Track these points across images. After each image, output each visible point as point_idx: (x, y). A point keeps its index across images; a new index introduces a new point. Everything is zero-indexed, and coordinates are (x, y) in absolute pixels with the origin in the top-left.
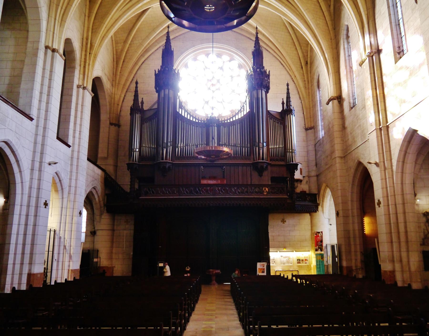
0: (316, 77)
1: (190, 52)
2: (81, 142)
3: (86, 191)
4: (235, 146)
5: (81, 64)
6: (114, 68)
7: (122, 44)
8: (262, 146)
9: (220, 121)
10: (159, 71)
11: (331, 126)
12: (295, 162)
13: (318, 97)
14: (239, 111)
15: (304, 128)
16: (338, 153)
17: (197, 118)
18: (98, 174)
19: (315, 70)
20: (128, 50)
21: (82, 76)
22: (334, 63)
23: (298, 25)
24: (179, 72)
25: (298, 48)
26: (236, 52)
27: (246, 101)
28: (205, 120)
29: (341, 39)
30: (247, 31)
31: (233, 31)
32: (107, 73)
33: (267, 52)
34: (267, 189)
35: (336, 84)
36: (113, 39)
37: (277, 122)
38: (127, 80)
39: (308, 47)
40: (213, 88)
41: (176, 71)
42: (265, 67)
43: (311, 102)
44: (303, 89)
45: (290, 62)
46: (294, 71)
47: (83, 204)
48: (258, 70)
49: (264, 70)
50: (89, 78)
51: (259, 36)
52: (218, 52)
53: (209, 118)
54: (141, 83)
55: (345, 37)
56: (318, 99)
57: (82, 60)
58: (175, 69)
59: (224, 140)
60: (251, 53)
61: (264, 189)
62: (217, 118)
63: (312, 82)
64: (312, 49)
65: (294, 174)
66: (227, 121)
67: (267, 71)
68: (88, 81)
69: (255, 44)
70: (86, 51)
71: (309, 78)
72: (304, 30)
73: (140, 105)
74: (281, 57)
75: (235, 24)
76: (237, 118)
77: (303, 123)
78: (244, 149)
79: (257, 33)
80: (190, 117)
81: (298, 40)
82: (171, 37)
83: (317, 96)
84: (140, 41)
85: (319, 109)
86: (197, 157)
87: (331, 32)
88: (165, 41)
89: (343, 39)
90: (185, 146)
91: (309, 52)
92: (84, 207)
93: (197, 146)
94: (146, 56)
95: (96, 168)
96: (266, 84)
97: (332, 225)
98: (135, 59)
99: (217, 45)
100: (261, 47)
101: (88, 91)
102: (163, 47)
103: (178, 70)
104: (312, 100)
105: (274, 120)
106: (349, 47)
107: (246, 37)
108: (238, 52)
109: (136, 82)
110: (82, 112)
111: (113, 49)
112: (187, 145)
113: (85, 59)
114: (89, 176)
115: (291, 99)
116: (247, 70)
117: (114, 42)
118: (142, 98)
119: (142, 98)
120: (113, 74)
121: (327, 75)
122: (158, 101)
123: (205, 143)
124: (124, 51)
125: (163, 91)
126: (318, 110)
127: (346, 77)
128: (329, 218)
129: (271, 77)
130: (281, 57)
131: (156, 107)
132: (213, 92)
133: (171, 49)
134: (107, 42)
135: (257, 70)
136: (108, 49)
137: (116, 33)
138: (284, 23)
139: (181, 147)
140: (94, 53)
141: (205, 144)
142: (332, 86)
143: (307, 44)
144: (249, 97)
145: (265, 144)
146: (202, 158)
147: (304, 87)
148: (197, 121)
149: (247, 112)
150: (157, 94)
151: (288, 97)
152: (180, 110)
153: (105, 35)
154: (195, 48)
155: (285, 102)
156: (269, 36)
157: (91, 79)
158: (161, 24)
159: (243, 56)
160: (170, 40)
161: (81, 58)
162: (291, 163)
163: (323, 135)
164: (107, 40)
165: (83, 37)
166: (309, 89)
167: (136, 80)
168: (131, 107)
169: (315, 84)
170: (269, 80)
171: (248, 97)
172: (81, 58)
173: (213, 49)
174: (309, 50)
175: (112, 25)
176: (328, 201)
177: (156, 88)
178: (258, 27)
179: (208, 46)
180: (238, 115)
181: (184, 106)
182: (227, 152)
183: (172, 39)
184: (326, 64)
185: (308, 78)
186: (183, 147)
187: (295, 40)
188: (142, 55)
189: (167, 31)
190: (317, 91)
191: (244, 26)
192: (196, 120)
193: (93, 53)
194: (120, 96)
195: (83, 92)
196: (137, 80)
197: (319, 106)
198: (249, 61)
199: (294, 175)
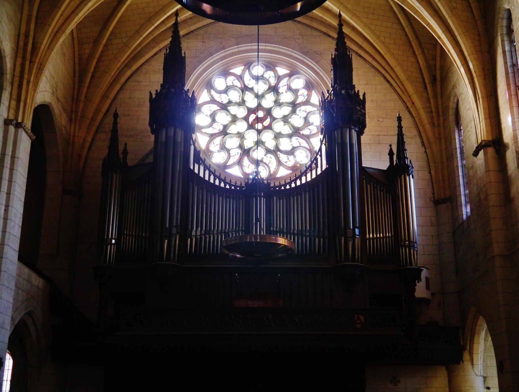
0: (452, 105)
1: (215, 59)
2: (8, 225)
3: (13, 319)
4: (301, 233)
5: (14, 80)
6: (74, 88)
7: (91, 45)
8: (351, 235)
9: (272, 187)
10: (157, 93)
11: (482, 196)
12: (416, 265)
13: (457, 141)
14: (307, 169)
15: (432, 199)
16: (497, 249)
17: (228, 180)
18: (38, 287)
19: (451, 92)
20: (101, 56)
21: (14, 103)
22: (485, 79)
23: (418, 11)
24: (194, 97)
25: (418, 52)
26: (302, 59)
27: (320, 150)
28: (243, 184)
29: (497, 34)
30: (322, 22)
31: (296, 21)
32: (60, 96)
33: (359, 58)
34: (362, 318)
35: (490, 118)
36: (75, 36)
37: (380, 188)
38: (97, 111)
39: (436, 50)
40: (259, 126)
41: (189, 94)
42: (356, 86)
43: (444, 152)
44: (428, 127)
45: (402, 77)
46: (410, 95)
47: (6, 346)
48: (343, 92)
49: (355, 91)
50: (27, 106)
51: (343, 30)
52: (269, 58)
53: (250, 182)
54: (124, 115)
55: (505, 31)
56: (458, 146)
57: (16, 74)
58: (188, 90)
59: (279, 222)
60: (330, 61)
61: (356, 318)
62: (266, 182)
63: (445, 114)
64: (443, 54)
65: (415, 289)
66: (285, 187)
67: (360, 94)
68: (26, 112)
69: (337, 45)
70: (24, 58)
71: (440, 106)
72: (427, 19)
73: (121, 156)
74: (387, 67)
75: (298, 9)
76: (304, 181)
77: (429, 191)
79: (341, 25)
80: (215, 180)
81: (417, 37)
82: (182, 33)
83: (455, 139)
84: (124, 40)
85: (460, 164)
86: (227, 255)
87: (479, 23)
88: (170, 39)
89: (502, 35)
90: (205, 235)
91: (438, 59)
92: (8, 351)
93: (227, 234)
94: (135, 67)
95: (34, 276)
96: (359, 118)
97: (492, 390)
98: (113, 73)
99: (266, 46)
100: (348, 50)
101: (24, 130)
102: (167, 50)
103: (193, 92)
104: (446, 148)
105: (373, 185)
106: (513, 49)
107: (320, 31)
108: (307, 59)
109: (114, 114)
110: (12, 169)
111: (74, 53)
112: (208, 232)
113: (22, 72)
114: (20, 292)
115: (407, 147)
116: (322, 93)
117: (76, 41)
118: (124, 143)
119: (126, 144)
120: (73, 100)
121: (474, 100)
122: (155, 150)
124: (95, 58)
125: (164, 131)
126: (458, 166)
127: (508, 104)
128: (485, 375)
129: (367, 105)
130: (387, 67)
131: (150, 159)
132: (259, 132)
133: (181, 54)
134: (63, 42)
135: (341, 92)
136: (64, 54)
137: (80, 26)
138: (391, 7)
139: (196, 236)
140: (39, 62)
141: (242, 231)
142: (484, 121)
143: (435, 43)
144: (325, 142)
145: (357, 231)
146: (236, 257)
147: (429, 123)
148: (228, 187)
149: (323, 169)
150: (153, 137)
151: (401, 143)
152: (196, 166)
153: (59, 29)
154: (225, 52)
155: (395, 151)
156: (363, 30)
157: (31, 108)
158: (163, 10)
159: (315, 66)
160: (179, 37)
161: (14, 70)
162: (409, 267)
163: (469, 214)
164: (63, 38)
165: (19, 32)
166: (439, 126)
167: (115, 109)
168: (104, 161)
169: (452, 118)
170: (365, 110)
171: (324, 142)
172: (14, 70)
173: (259, 54)
174: (438, 54)
175: (73, 12)
176: (482, 342)
177: (151, 124)
178: (342, 13)
179: (250, 48)
180: (306, 176)
181: (203, 158)
182: (285, 246)
183: (184, 36)
184: (471, 81)
185: (437, 107)
186: (201, 235)
187: (411, 37)
188: (128, 65)
189: (174, 22)
190: (454, 130)
191: (316, 12)
192: (225, 185)
193: (37, 61)
194: (84, 141)
195: (15, 132)
196: (116, 111)
197: (459, 159)
198: (325, 76)
199: (414, 290)
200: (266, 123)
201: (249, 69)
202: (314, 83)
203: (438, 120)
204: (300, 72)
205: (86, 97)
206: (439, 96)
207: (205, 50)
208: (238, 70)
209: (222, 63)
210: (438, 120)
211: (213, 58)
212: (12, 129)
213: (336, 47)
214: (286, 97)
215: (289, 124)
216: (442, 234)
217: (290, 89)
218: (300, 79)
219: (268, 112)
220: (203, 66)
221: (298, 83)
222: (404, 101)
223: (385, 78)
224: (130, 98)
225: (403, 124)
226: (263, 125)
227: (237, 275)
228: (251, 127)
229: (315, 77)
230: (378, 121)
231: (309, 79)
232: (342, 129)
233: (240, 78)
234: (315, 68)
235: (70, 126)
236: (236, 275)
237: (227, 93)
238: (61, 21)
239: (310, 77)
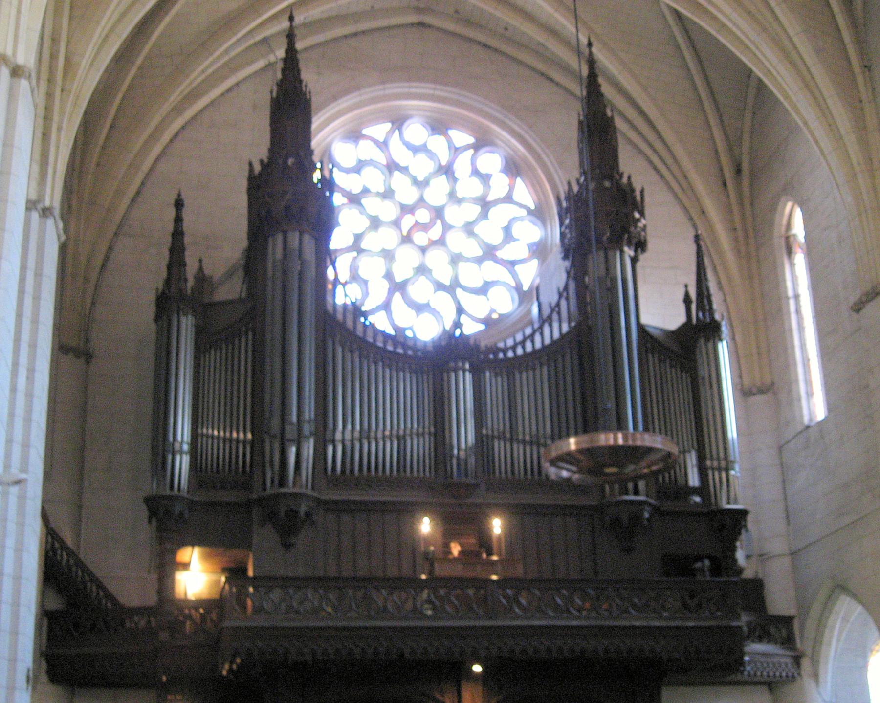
112: (365, 435)
125: (280, 237)
148: (400, 351)
186: (352, 441)
200: (436, 232)
203: (747, 244)
205: (98, 165)
210: (747, 244)
212: (35, 216)
214: (469, 187)
217: (476, 172)
219: (438, 213)
223: (651, 162)
228: (407, 239)
232: (606, 251)
233: (383, 145)
238: (116, 15)
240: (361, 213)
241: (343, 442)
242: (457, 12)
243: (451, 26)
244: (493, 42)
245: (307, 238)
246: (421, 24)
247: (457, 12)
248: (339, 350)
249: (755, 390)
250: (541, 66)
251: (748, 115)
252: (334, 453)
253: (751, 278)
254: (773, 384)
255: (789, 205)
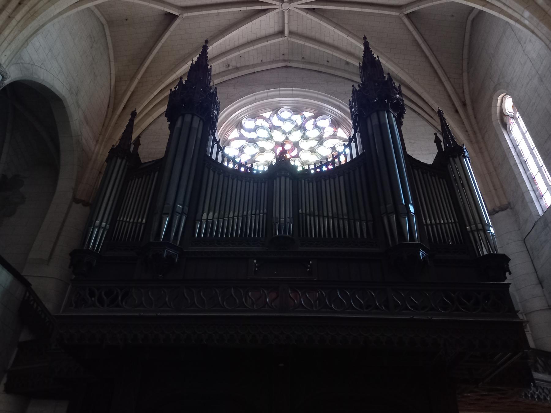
78: (358, 224)
123: (265, 210)
186: (213, 219)
201: (277, 113)
202: (340, 120)
204: (325, 113)
206: (472, 117)
207: (236, 94)
208: (267, 115)
209: (252, 107)
211: (243, 100)
213: (364, 53)
215: (316, 153)
216: (508, 244)
218: (326, 119)
219: (296, 145)
220: (233, 105)
221: (324, 122)
222: (434, 126)
224: (161, 129)
225: (445, 116)
226: (290, 155)
227: (255, 261)
229: (340, 115)
230: (410, 142)
231: (335, 117)
234: (341, 105)
235: (95, 146)
236: (254, 261)
237: (256, 131)
239: (336, 116)
240: (255, 148)
241: (207, 220)
242: (303, 58)
243: (301, 66)
244: (322, 69)
245: (196, 120)
246: (286, 67)
247: (303, 58)
248: (212, 173)
249: (497, 209)
250: (347, 76)
251: (465, 74)
252: (200, 229)
253: (482, 153)
254: (509, 203)
255: (500, 98)
